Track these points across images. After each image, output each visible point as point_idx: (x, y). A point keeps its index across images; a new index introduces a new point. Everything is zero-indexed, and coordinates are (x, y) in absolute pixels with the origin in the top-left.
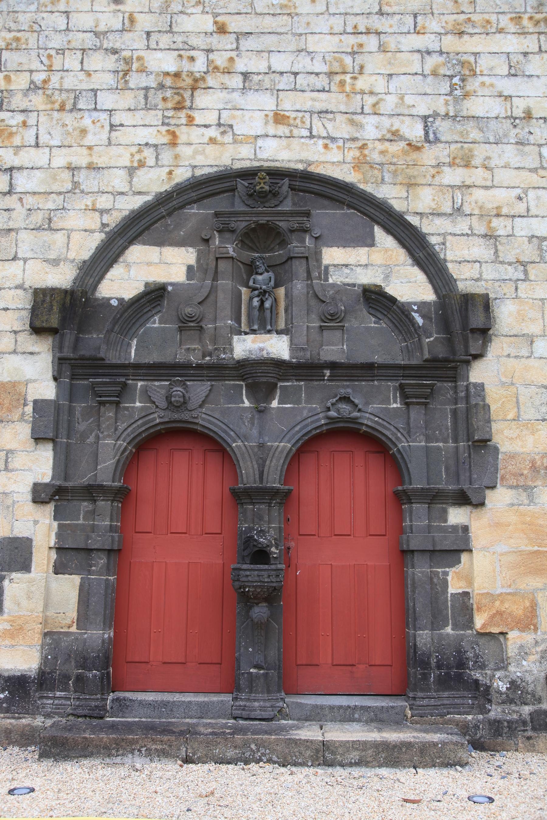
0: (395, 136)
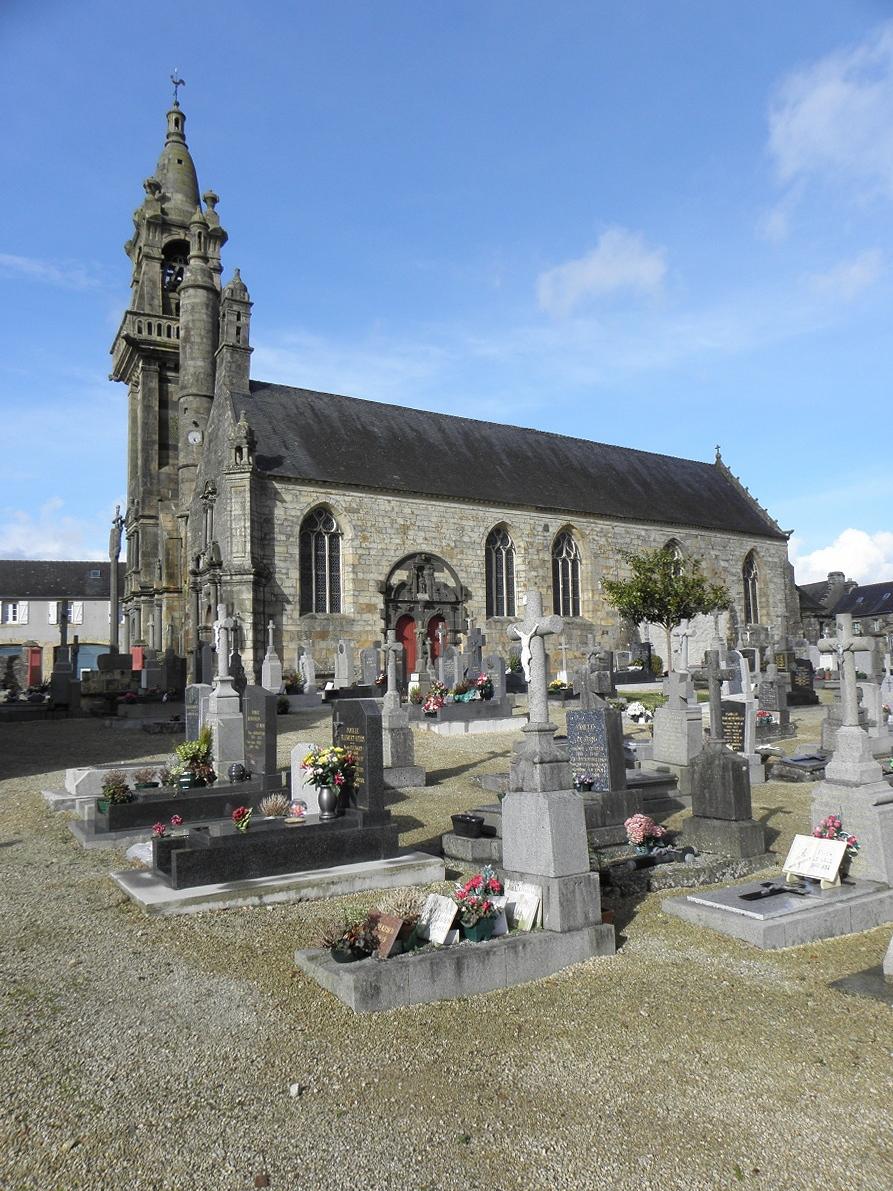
0: (449, 545)
